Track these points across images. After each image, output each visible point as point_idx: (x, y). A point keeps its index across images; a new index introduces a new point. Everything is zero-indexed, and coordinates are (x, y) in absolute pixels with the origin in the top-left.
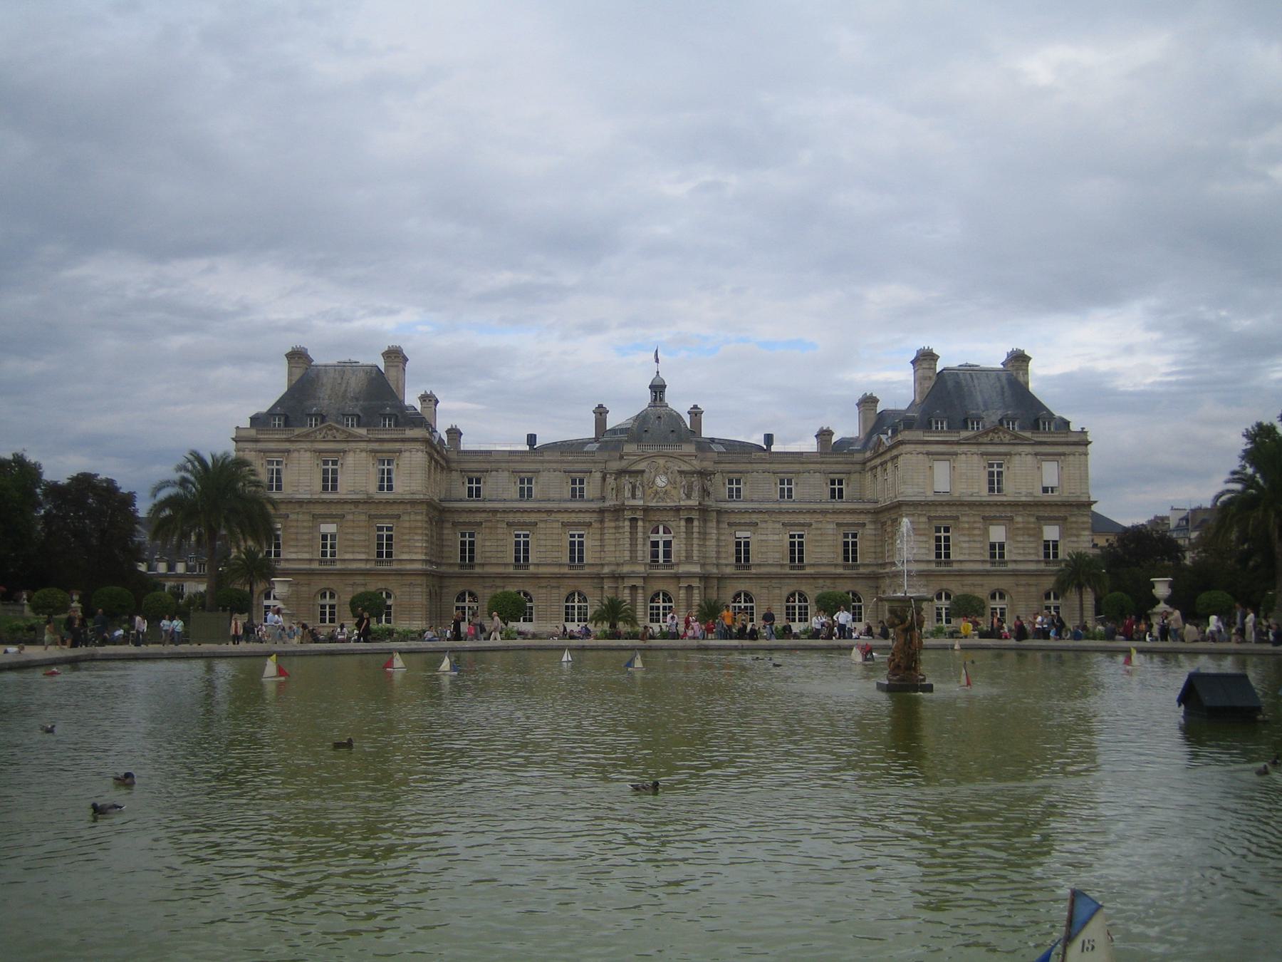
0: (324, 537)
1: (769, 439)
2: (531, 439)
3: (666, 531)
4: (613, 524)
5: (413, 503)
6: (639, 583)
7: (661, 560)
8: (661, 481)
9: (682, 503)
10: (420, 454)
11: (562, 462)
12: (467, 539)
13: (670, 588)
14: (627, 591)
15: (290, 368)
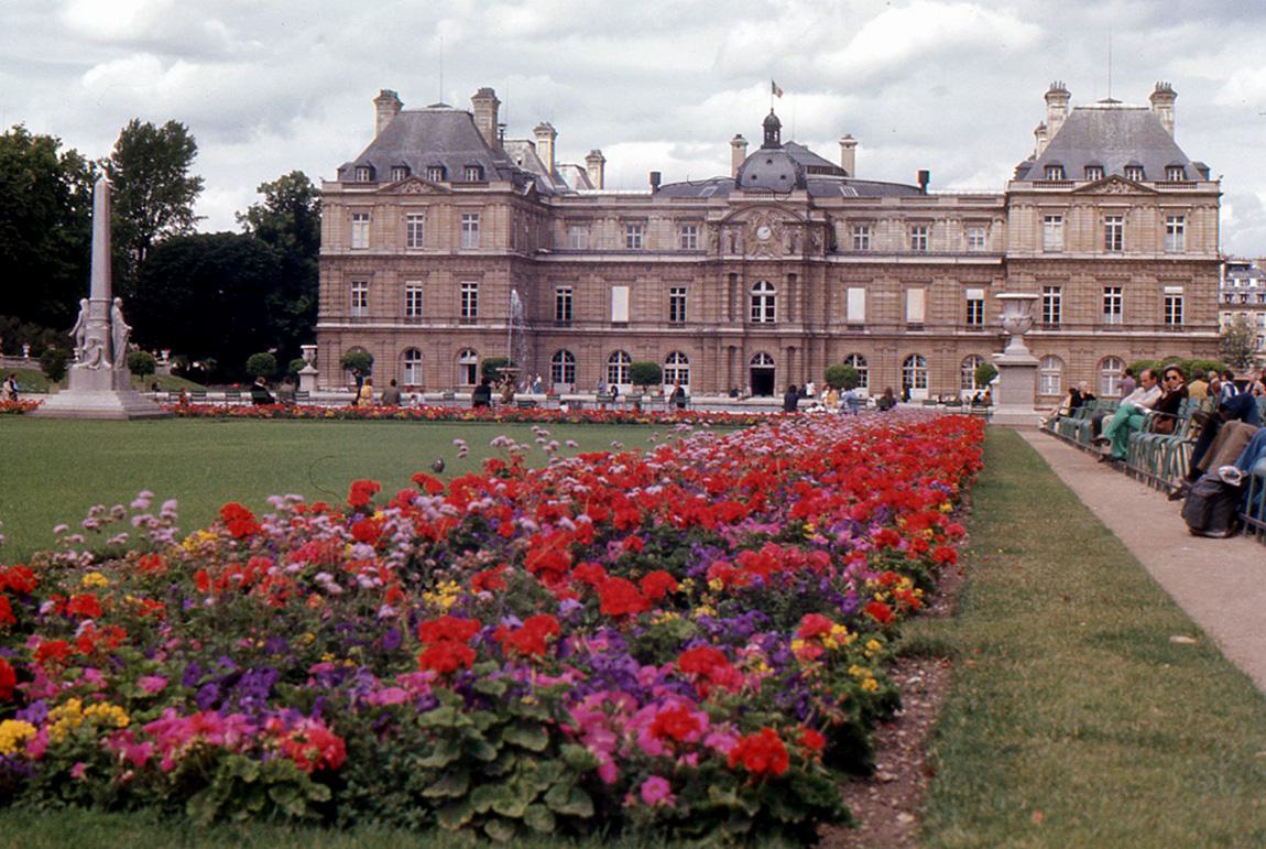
0: (410, 294)
1: (924, 177)
2: (655, 177)
3: (769, 287)
4: (713, 279)
5: (497, 258)
6: (737, 343)
7: (763, 318)
8: (764, 233)
9: (785, 258)
10: (504, 208)
11: (672, 208)
12: (564, 295)
13: (773, 350)
14: (725, 352)
15: (379, 114)
